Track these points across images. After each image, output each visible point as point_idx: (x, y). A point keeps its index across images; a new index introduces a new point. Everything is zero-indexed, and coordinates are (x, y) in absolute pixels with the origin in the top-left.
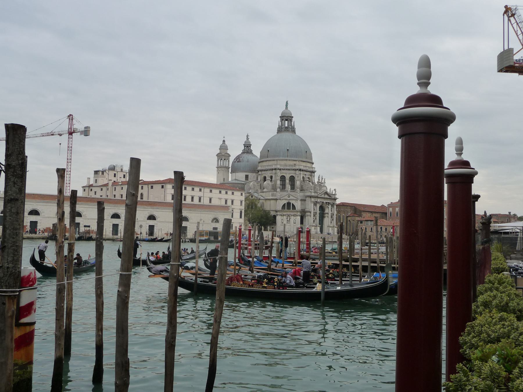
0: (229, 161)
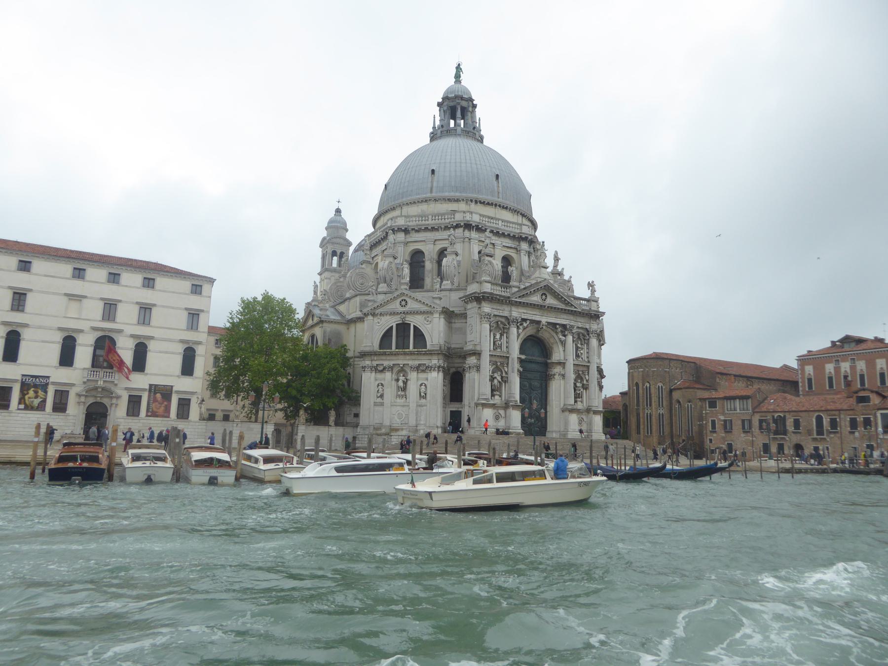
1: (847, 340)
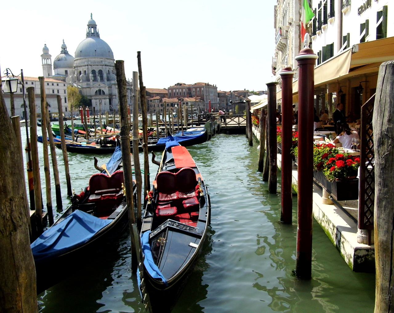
0: (51, 60)
1: (178, 84)
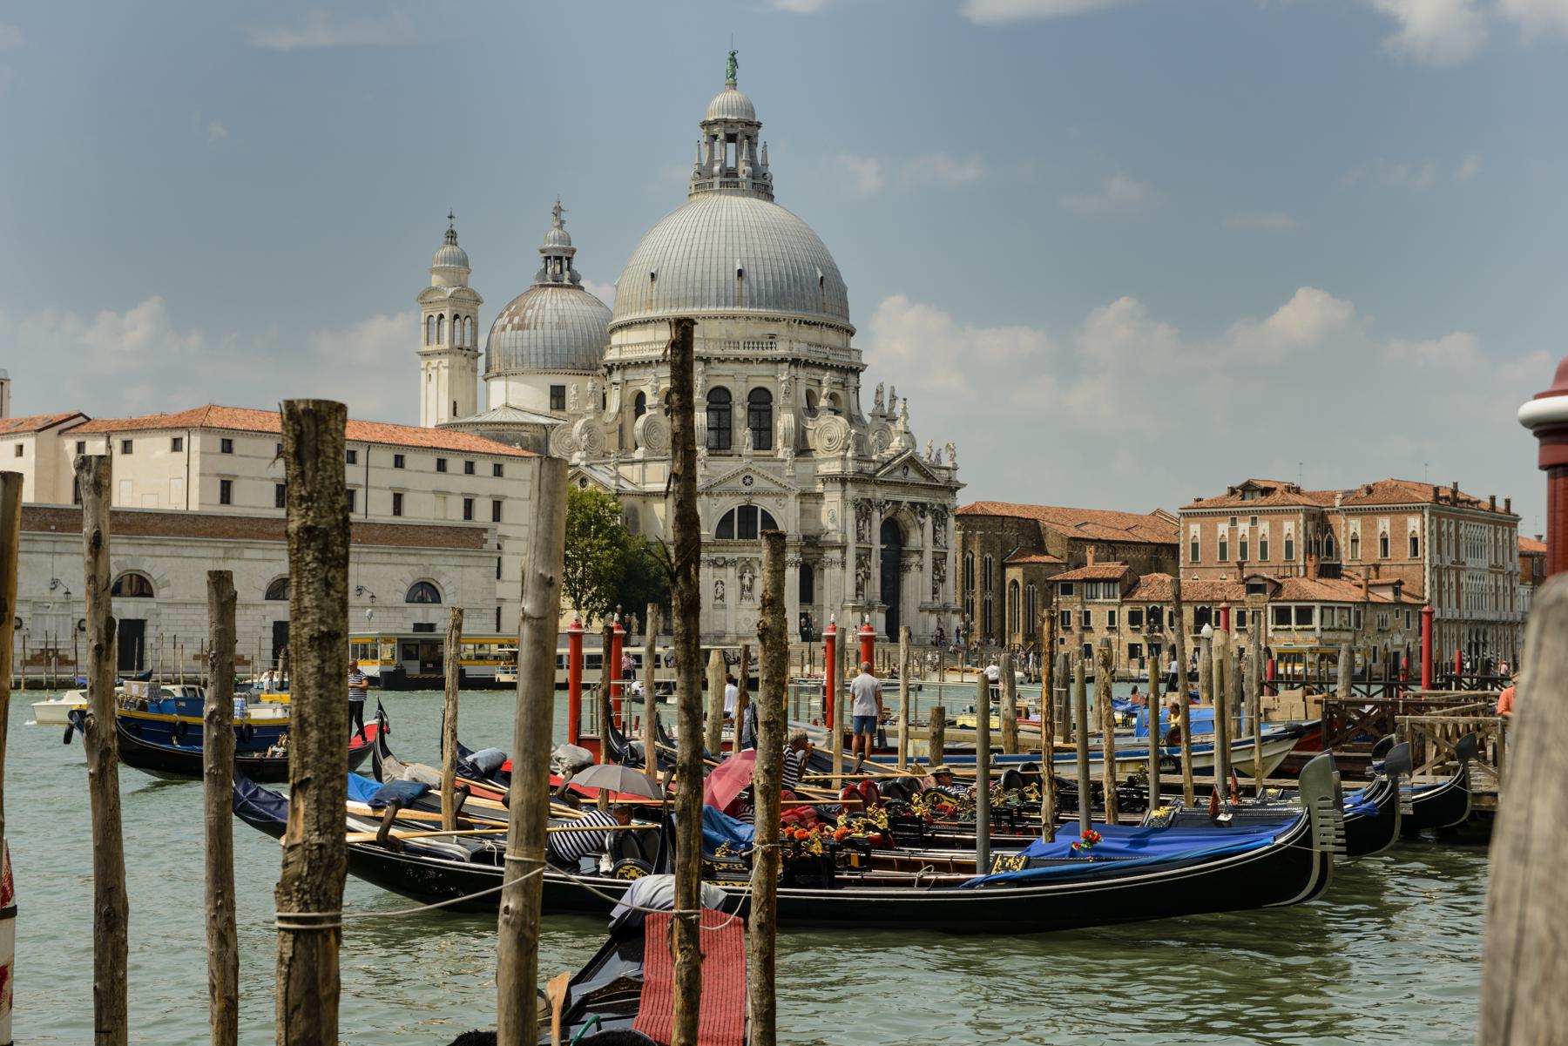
0: (475, 325)
1: (1248, 488)
